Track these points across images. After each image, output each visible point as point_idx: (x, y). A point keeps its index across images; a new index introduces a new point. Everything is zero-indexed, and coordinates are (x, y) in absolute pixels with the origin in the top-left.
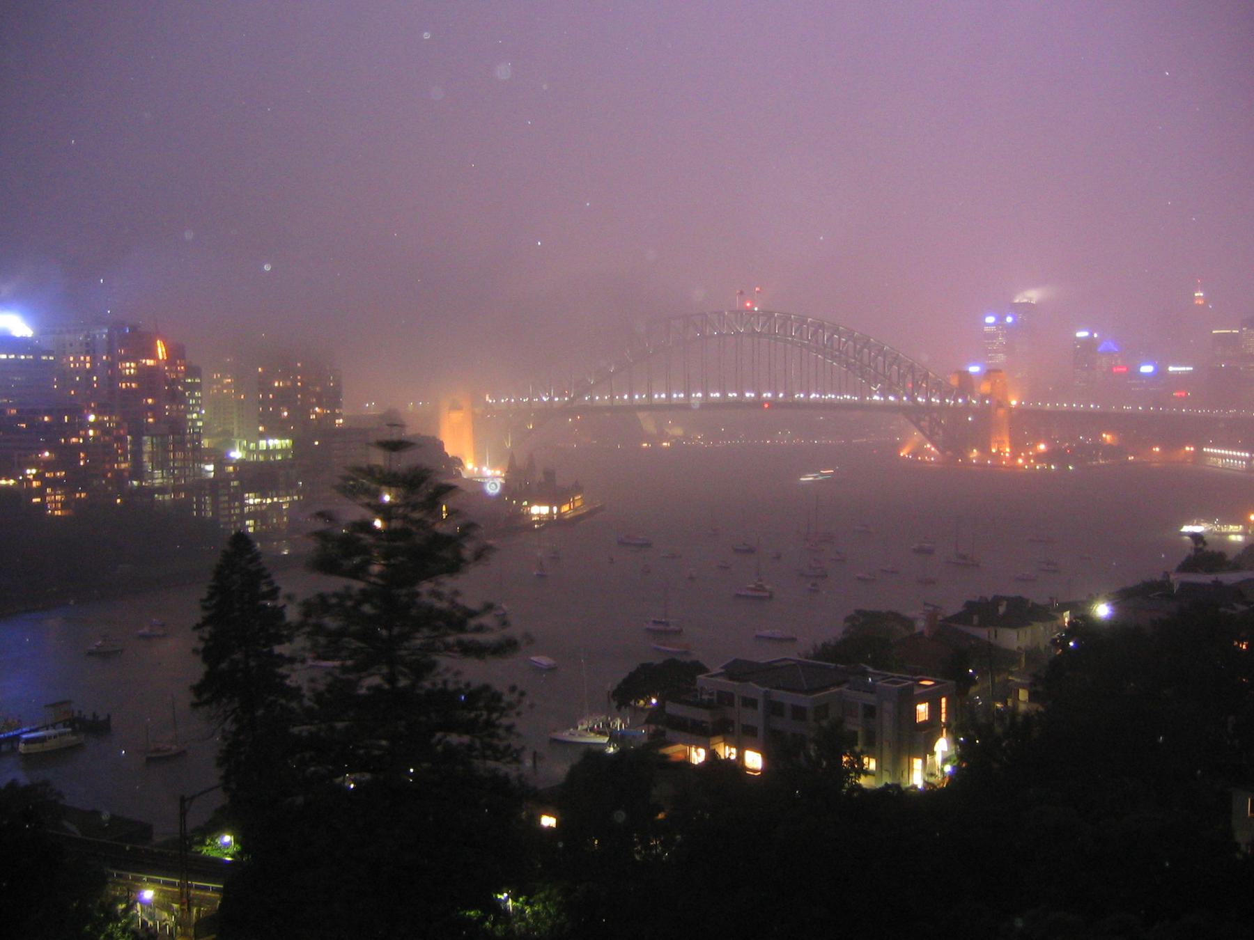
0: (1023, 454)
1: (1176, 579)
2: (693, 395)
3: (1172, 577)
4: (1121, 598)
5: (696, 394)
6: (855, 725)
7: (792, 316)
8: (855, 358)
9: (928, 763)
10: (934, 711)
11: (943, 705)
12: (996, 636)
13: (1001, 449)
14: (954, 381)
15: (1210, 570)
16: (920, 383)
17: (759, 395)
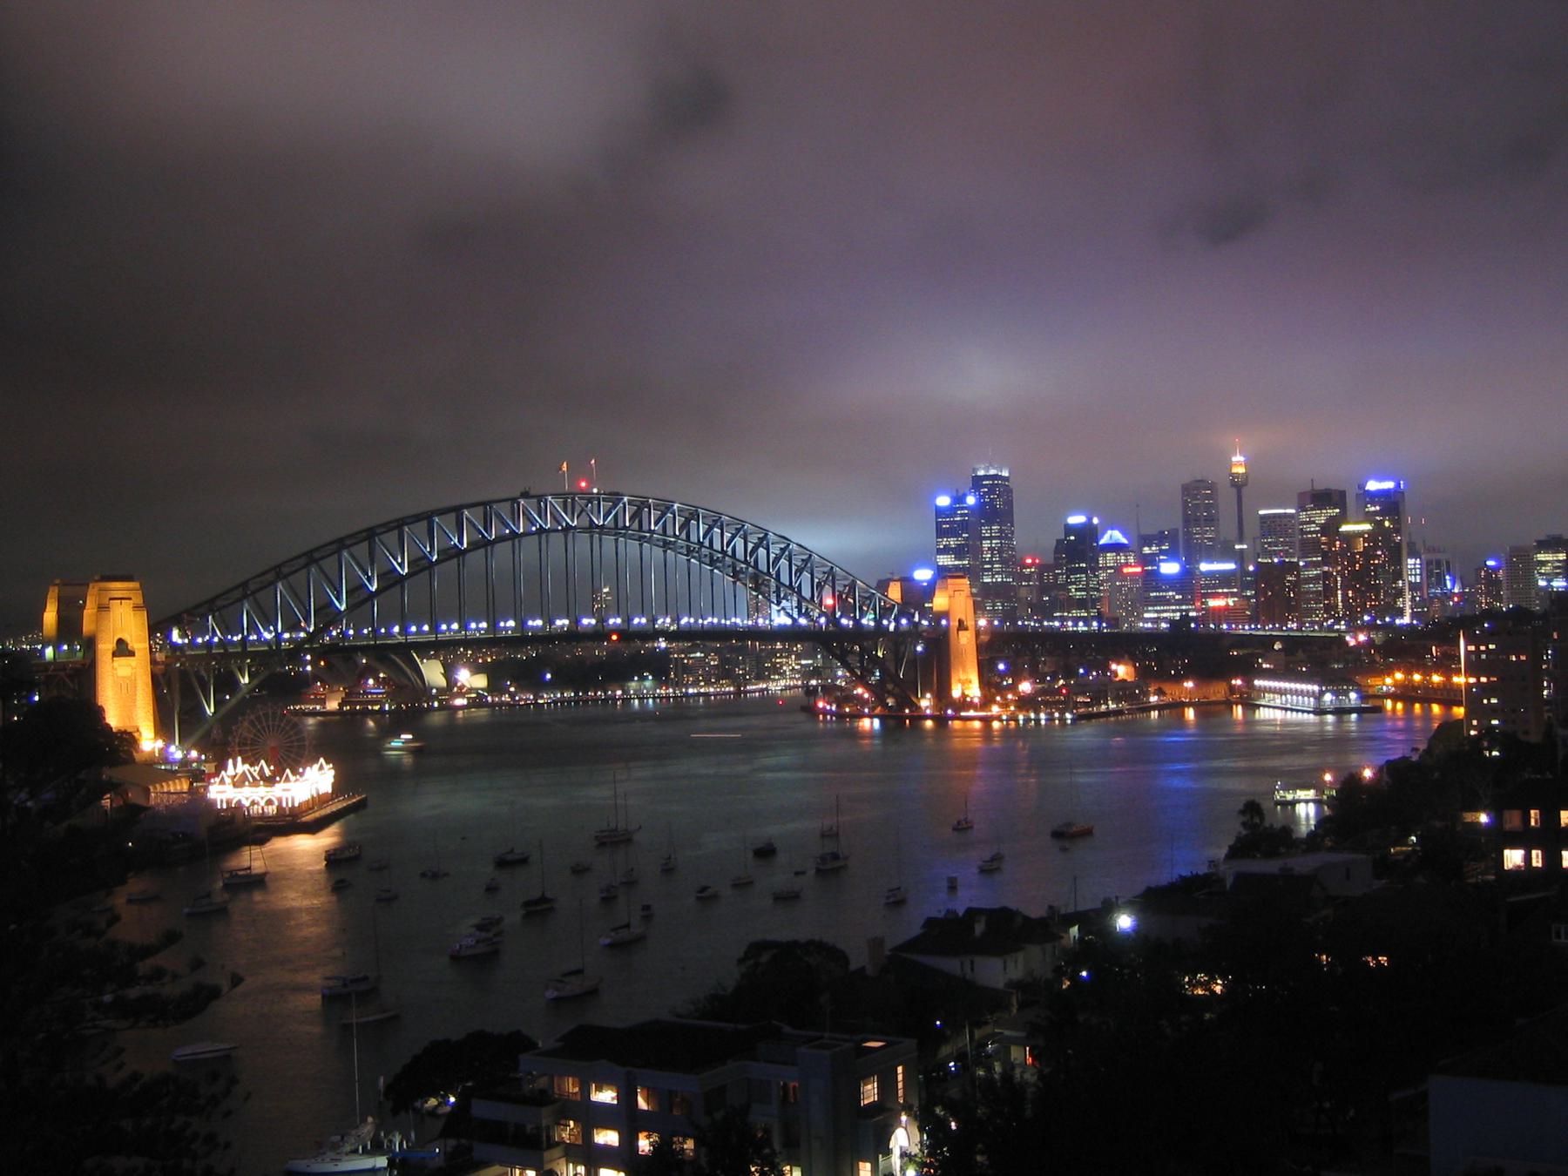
0: (998, 698)
1: (1228, 872)
2: (502, 624)
3: (1222, 868)
4: (1149, 902)
5: (505, 622)
6: (764, 1118)
7: (650, 501)
8: (745, 562)
9: (881, 1168)
10: (887, 1087)
11: (900, 1077)
12: (972, 969)
13: (967, 692)
14: (895, 592)
15: (1271, 854)
16: (844, 596)
17: (602, 620)
